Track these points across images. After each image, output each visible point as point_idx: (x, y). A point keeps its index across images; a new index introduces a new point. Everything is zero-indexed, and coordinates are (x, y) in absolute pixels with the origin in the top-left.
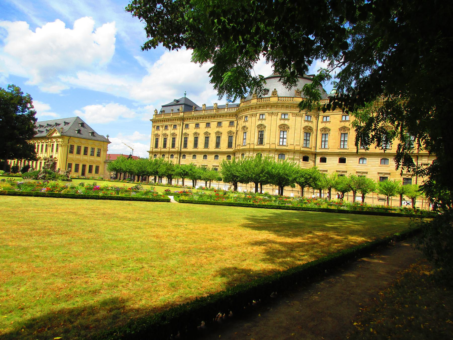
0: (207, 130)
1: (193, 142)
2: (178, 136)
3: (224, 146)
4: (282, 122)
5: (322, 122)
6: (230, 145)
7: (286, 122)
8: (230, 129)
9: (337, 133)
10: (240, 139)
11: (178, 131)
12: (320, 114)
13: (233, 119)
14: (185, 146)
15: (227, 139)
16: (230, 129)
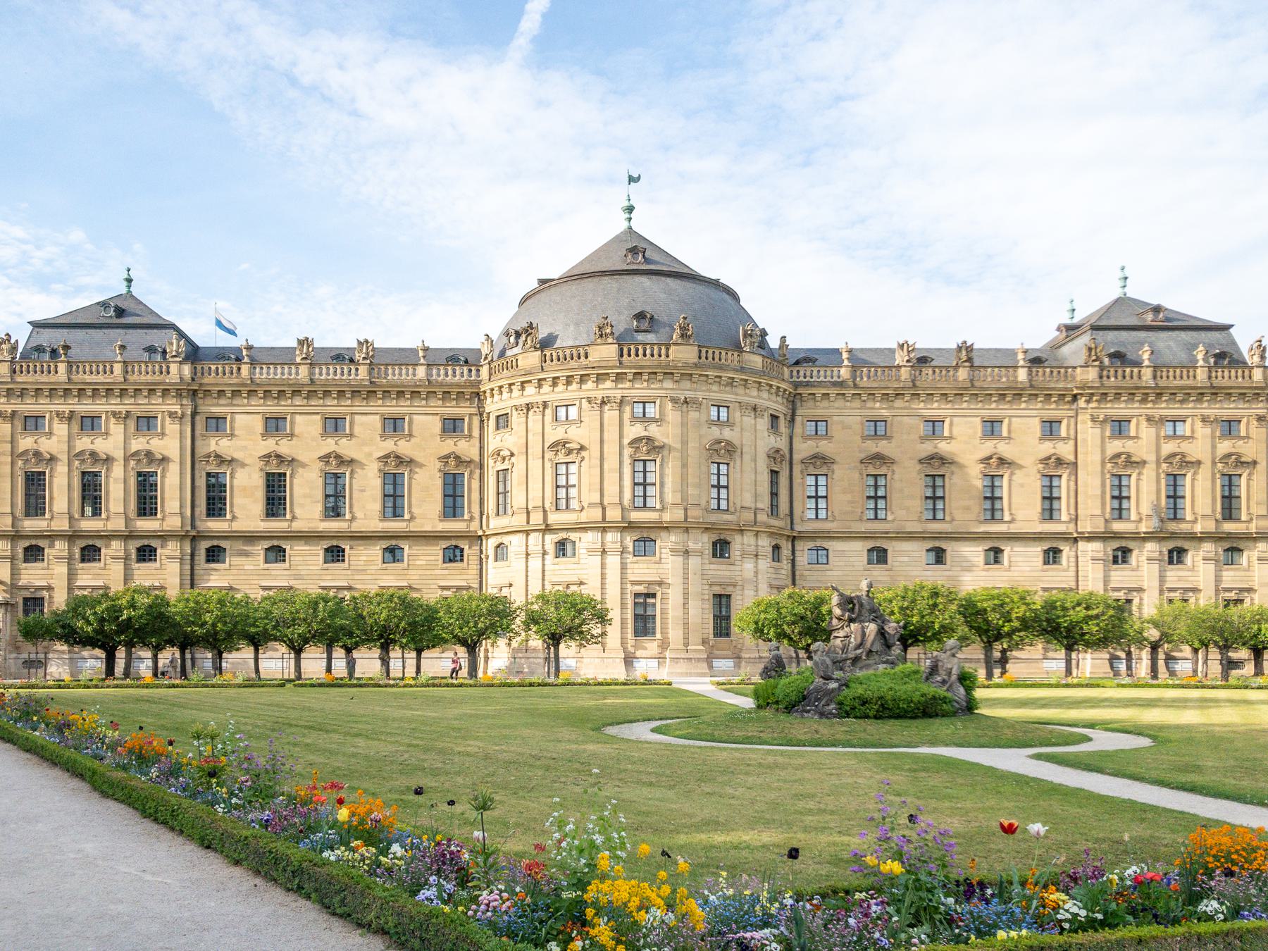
0: (329, 445)
1: (260, 494)
2: (174, 468)
3: (425, 506)
4: (715, 432)
5: (806, 438)
6: (452, 502)
7: (727, 434)
8: (449, 446)
9: (857, 475)
10: (535, 485)
11: (169, 442)
12: (799, 412)
13: (464, 410)
14: (216, 505)
15: (439, 482)
16: (449, 446)
